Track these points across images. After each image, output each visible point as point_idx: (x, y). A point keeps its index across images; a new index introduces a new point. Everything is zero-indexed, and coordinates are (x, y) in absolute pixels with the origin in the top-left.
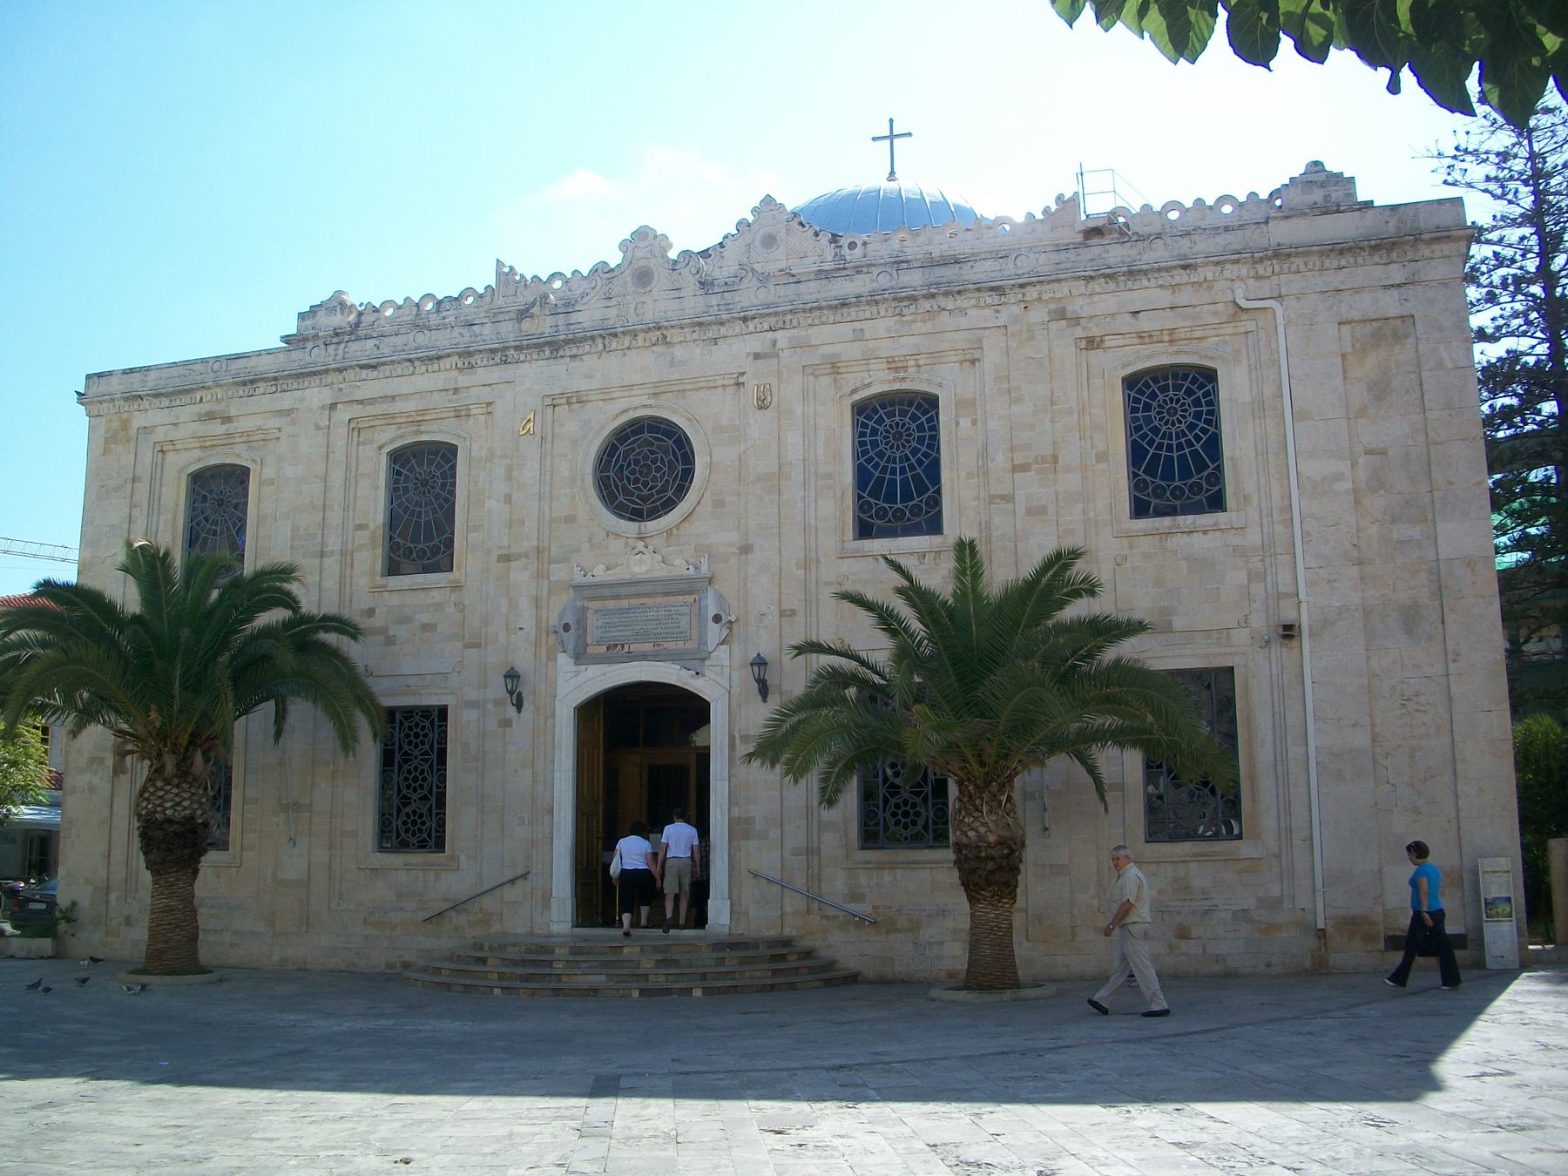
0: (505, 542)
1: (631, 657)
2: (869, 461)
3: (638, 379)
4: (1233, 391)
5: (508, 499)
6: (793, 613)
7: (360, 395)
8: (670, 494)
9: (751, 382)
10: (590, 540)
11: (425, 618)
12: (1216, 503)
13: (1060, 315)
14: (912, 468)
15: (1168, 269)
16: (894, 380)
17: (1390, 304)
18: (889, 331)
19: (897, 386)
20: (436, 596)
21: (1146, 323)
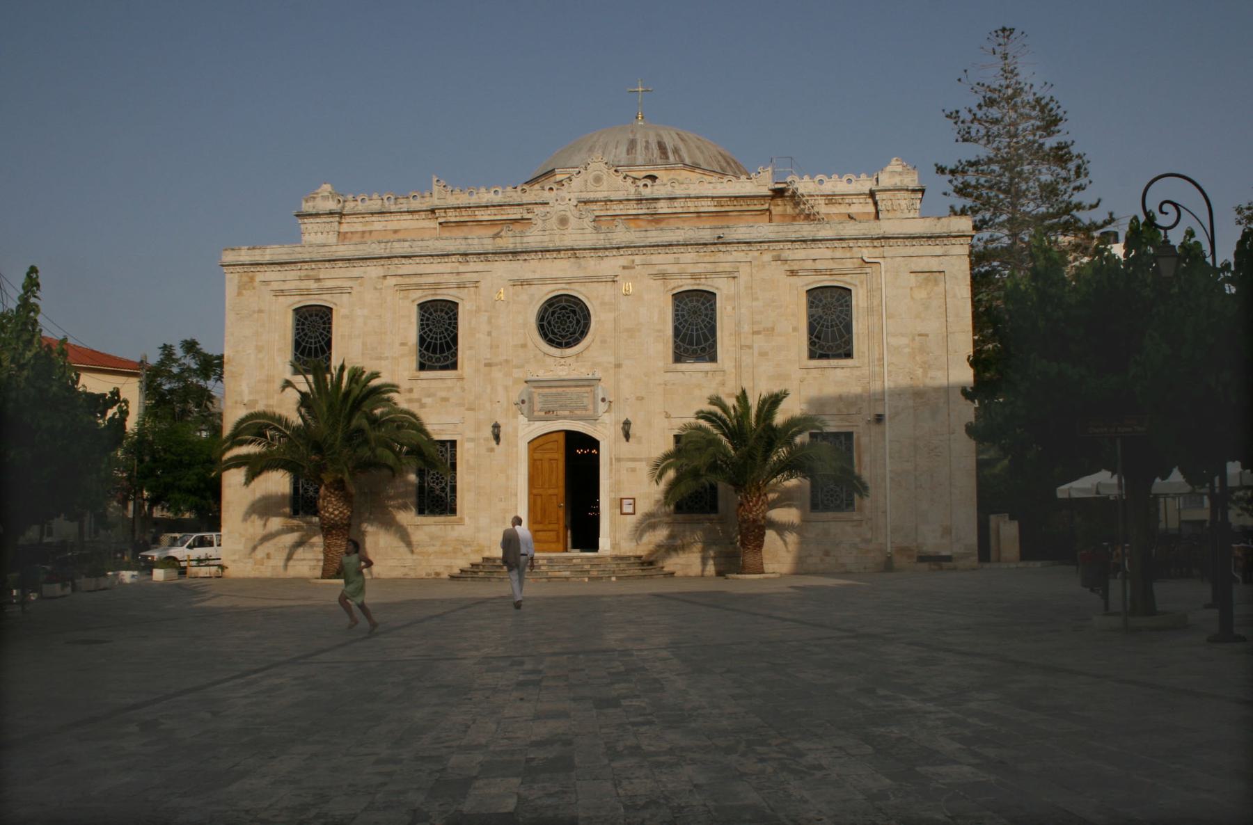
0: (489, 356)
1: (558, 418)
2: (680, 324)
3: (560, 275)
4: (859, 301)
5: (489, 334)
7: (400, 272)
8: (577, 335)
10: (535, 357)
11: (444, 394)
12: (849, 355)
13: (777, 258)
14: (701, 328)
15: (831, 240)
16: (694, 284)
17: (934, 264)
18: (693, 259)
19: (695, 288)
20: (449, 383)
21: (819, 265)
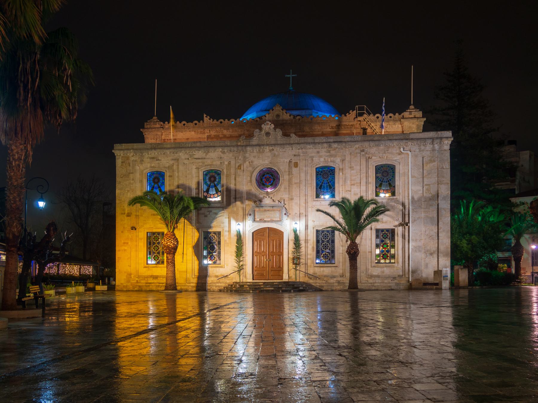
6: (302, 214)
7: (196, 157)
9: (293, 161)
19: (326, 165)
